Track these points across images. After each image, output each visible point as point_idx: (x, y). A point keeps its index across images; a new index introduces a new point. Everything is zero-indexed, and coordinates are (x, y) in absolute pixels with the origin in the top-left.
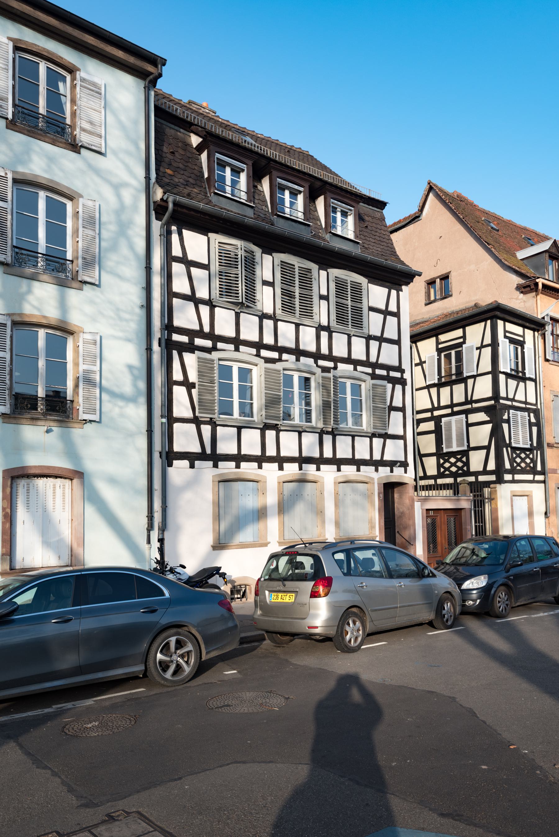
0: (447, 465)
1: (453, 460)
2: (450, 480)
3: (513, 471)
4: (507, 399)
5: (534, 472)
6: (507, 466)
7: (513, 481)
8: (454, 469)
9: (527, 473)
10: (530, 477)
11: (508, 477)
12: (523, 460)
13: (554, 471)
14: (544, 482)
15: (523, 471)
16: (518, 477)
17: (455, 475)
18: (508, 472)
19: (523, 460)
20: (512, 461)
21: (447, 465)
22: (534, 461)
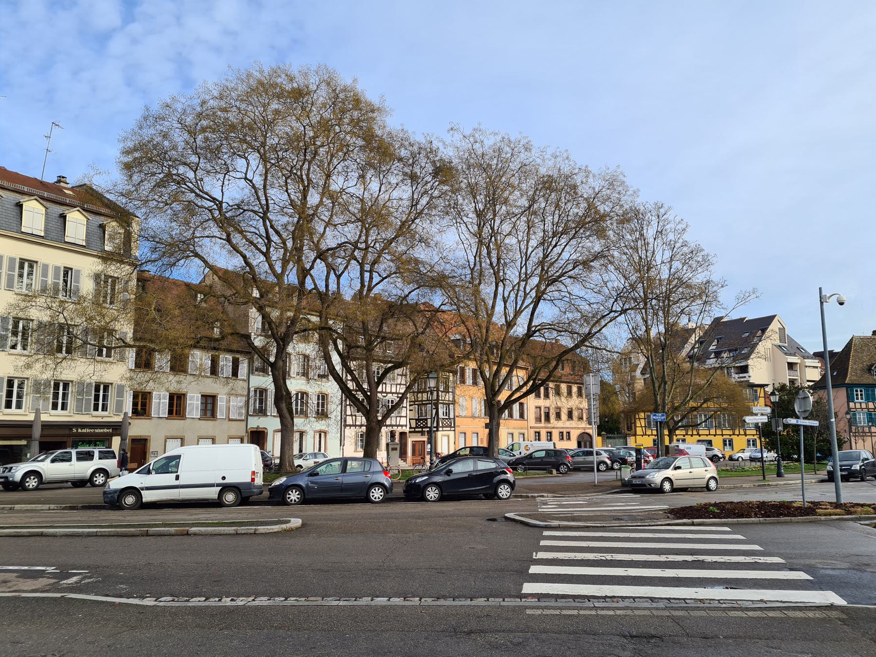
0: (419, 424)
1: (422, 422)
2: (421, 430)
3: (443, 427)
4: (442, 400)
5: (450, 426)
6: (441, 425)
7: (443, 430)
8: (422, 425)
9: (448, 427)
10: (449, 429)
11: (440, 429)
12: (447, 423)
13: (459, 426)
14: (454, 430)
15: (446, 427)
16: (444, 429)
17: (422, 428)
18: (441, 427)
19: (447, 423)
20: (442, 423)
21: (419, 424)
22: (451, 423)
